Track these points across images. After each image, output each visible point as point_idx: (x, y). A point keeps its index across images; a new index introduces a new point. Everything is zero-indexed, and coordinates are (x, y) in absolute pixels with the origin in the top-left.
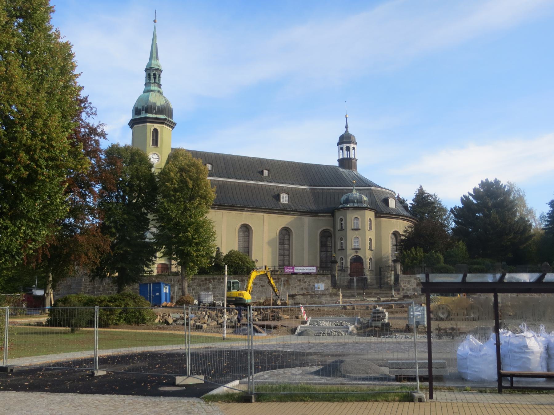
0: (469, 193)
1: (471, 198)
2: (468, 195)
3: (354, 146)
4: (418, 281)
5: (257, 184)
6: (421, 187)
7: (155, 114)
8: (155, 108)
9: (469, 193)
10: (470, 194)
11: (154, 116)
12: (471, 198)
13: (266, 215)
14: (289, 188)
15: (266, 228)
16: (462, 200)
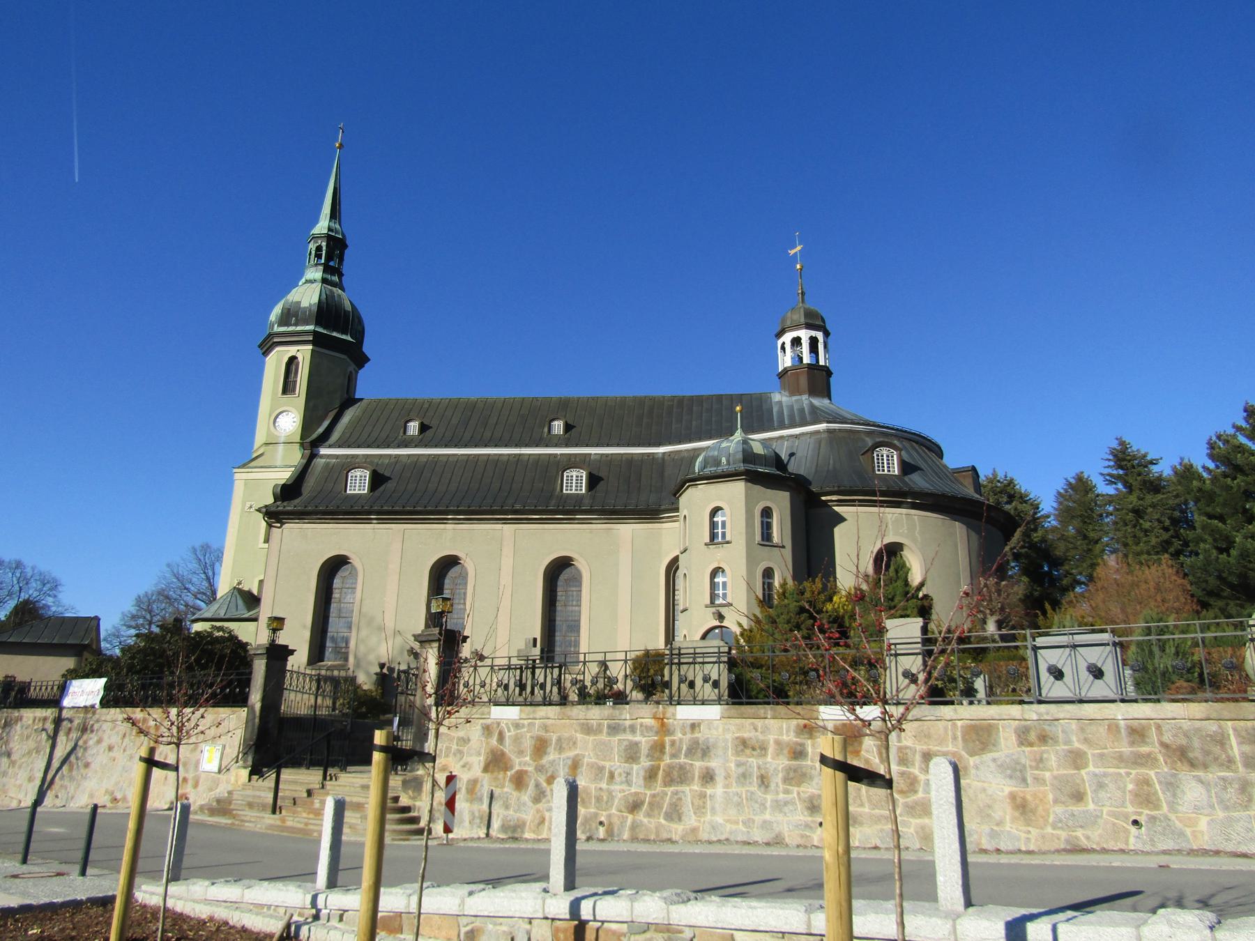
0: (1234, 426)
1: (1242, 439)
2: (1231, 431)
3: (820, 336)
4: (494, 741)
5: (520, 455)
6: (1122, 443)
7: (296, 325)
8: (298, 312)
9: (1234, 426)
10: (1239, 429)
11: (291, 329)
12: (1242, 439)
13: (508, 529)
14: (607, 455)
15: (507, 562)
16: (1212, 446)
